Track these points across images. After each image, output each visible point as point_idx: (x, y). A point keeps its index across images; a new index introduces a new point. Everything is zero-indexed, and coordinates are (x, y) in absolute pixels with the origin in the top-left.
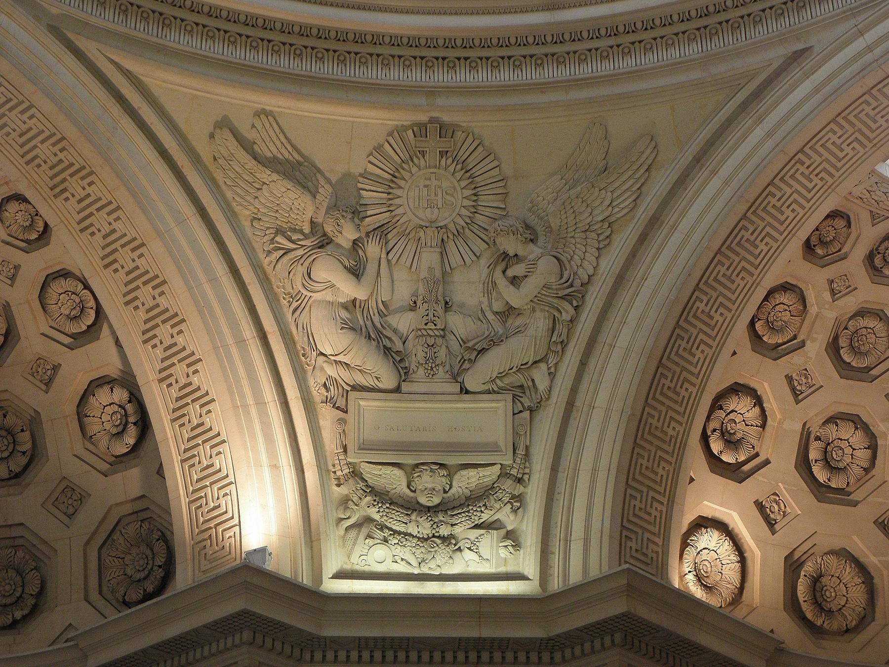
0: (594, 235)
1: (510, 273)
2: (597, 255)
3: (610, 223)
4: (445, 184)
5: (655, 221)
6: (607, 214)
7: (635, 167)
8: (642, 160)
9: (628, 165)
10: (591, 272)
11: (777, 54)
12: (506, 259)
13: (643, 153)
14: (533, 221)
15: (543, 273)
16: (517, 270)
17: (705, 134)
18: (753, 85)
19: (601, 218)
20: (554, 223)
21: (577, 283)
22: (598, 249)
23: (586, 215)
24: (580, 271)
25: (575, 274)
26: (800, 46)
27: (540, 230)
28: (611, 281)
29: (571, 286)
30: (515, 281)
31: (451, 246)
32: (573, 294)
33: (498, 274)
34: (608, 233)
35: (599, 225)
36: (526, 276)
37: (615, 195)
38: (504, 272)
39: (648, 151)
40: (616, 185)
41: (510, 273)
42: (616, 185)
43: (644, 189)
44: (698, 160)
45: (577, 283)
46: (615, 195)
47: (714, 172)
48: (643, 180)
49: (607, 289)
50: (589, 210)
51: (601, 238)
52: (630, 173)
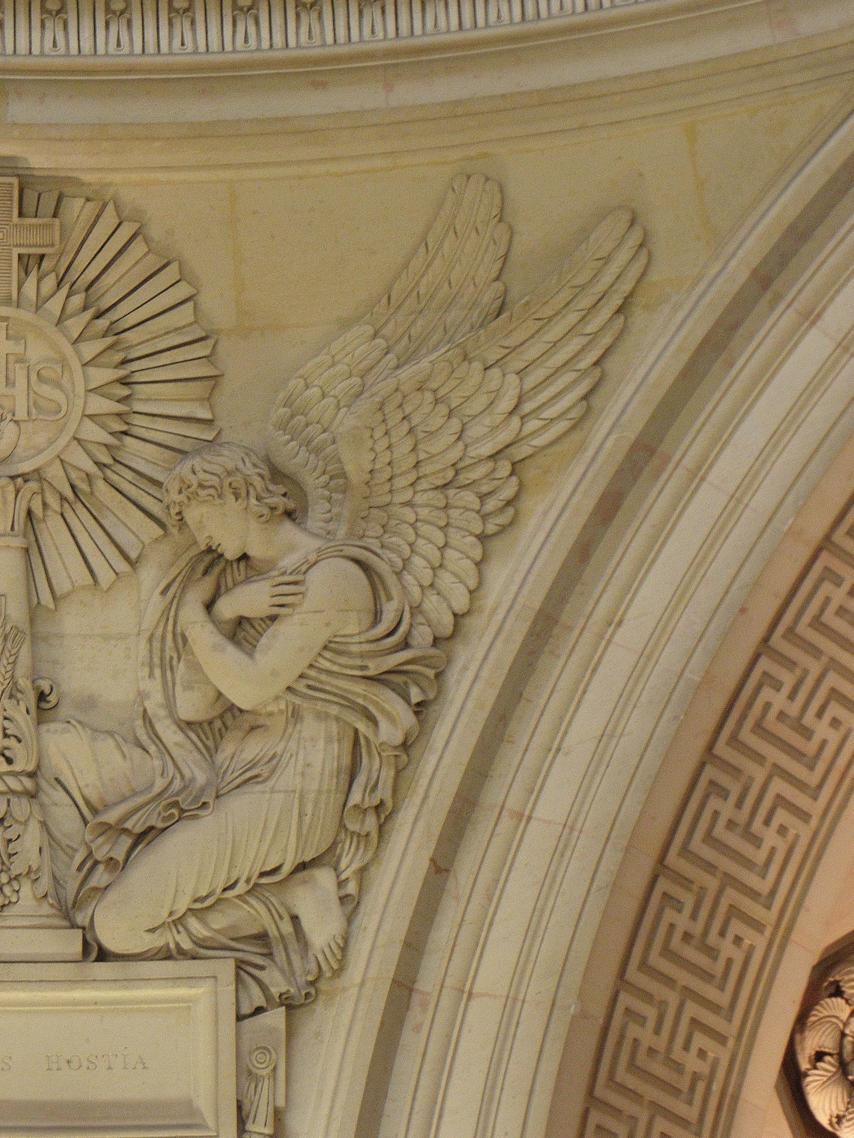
0: (469, 498)
1: (228, 608)
2: (477, 554)
4: (37, 351)
6: (503, 437)
7: (585, 302)
8: (607, 279)
9: (565, 295)
10: (461, 603)
12: (217, 569)
13: (607, 260)
14: (293, 457)
15: (325, 606)
16: (247, 599)
19: (487, 449)
20: (355, 464)
21: (422, 636)
22: (483, 538)
24: (432, 603)
25: (416, 609)
27: (313, 483)
28: (518, 631)
29: (405, 645)
30: (241, 632)
31: (53, 532)
32: (412, 669)
33: (192, 613)
34: (508, 492)
36: (273, 618)
37: (531, 381)
38: (209, 606)
39: (622, 257)
40: (532, 352)
41: (228, 608)
42: (532, 352)
43: (612, 364)
45: (422, 636)
46: (531, 381)
49: (506, 653)
50: (455, 425)
51: (491, 504)
52: (573, 318)
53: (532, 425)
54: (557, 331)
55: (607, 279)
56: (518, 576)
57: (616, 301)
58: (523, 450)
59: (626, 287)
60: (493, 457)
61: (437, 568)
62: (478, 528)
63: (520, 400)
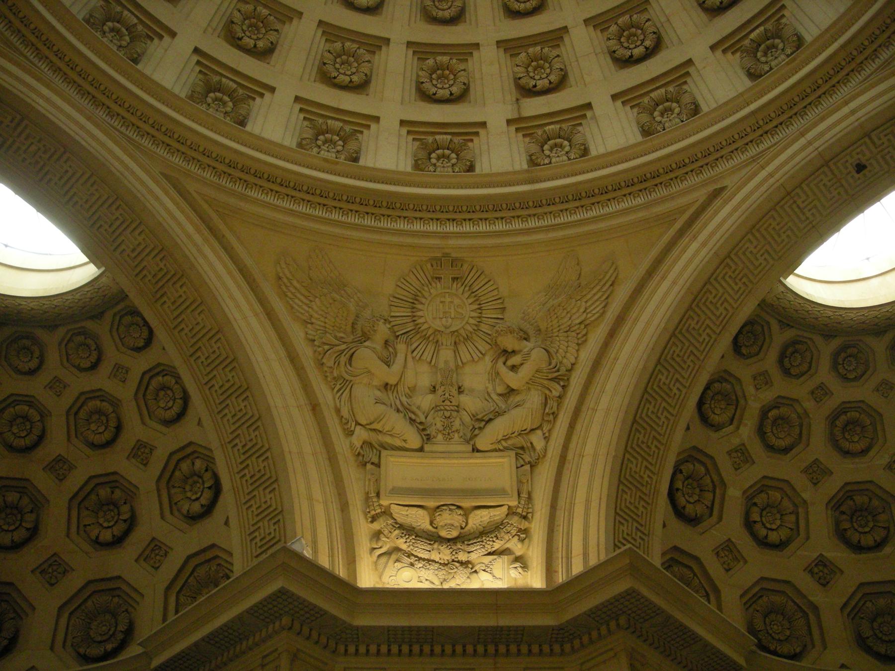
0: (574, 334)
2: (577, 348)
3: (586, 325)
5: (620, 320)
6: (583, 318)
7: (602, 284)
8: (607, 278)
9: (597, 282)
10: (573, 360)
11: (701, 195)
13: (607, 273)
16: (515, 360)
17: (654, 253)
18: (686, 216)
19: (578, 321)
20: (543, 326)
21: (563, 370)
22: (578, 344)
23: (565, 320)
24: (565, 361)
25: (561, 363)
26: (718, 186)
27: (531, 332)
28: (590, 364)
29: (558, 371)
30: (514, 368)
31: (462, 348)
32: (562, 378)
34: (584, 332)
35: (577, 327)
36: (522, 364)
37: (589, 304)
38: (504, 364)
39: (611, 271)
40: (589, 296)
41: (509, 363)
42: (589, 296)
43: (610, 300)
44: (650, 274)
45: (563, 370)
46: (589, 304)
47: (663, 278)
48: (608, 293)
50: (569, 315)
51: (580, 336)
52: (598, 287)
53: (589, 315)
54: (595, 290)
55: (607, 278)
56: (587, 354)
57: (610, 283)
58: (588, 322)
59: (613, 278)
60: (580, 323)
61: (566, 352)
62: (576, 341)
63: (586, 309)
